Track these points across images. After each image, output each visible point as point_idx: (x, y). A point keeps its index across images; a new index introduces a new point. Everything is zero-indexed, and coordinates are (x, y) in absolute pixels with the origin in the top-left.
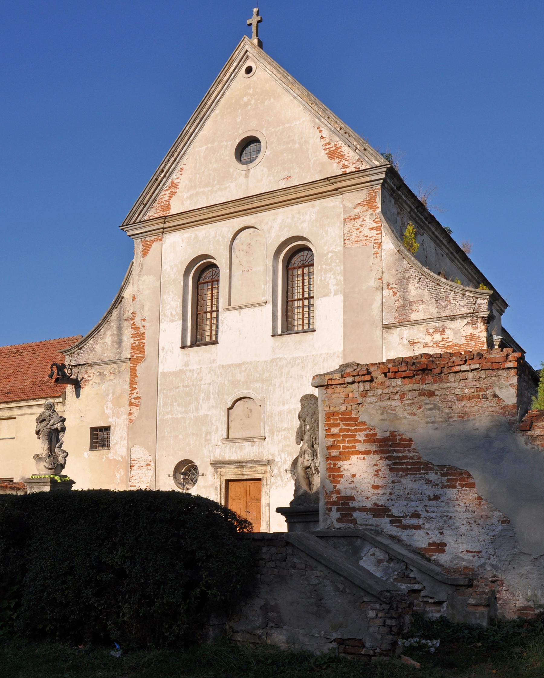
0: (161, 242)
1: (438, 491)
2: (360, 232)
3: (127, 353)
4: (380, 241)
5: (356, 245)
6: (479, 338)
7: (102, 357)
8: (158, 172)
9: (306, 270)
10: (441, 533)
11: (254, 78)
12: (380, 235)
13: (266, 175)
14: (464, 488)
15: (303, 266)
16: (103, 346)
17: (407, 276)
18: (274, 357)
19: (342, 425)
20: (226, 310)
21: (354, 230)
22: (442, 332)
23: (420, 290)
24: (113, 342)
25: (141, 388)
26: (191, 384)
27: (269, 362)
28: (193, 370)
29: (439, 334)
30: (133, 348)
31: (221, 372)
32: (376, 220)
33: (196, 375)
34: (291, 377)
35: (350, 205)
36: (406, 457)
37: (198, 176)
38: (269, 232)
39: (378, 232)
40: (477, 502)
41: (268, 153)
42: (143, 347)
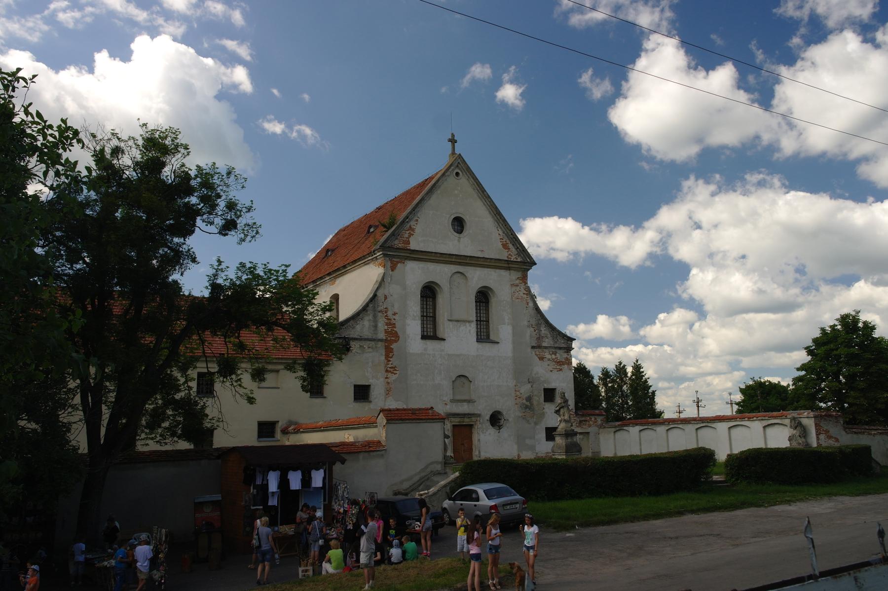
3: (382, 335)
16: (363, 328)
25: (394, 361)
30: (386, 331)
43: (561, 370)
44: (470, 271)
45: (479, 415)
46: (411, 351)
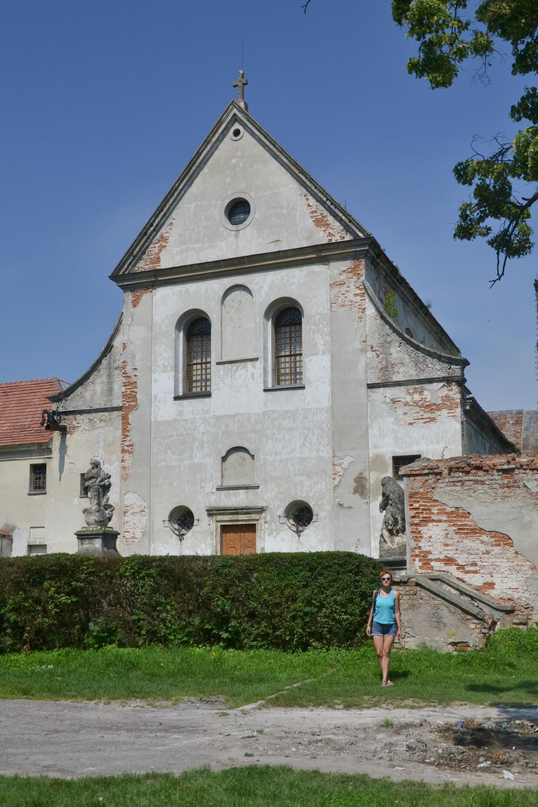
0: (151, 294)
1: (489, 548)
2: (346, 297)
4: (364, 307)
5: (342, 309)
6: (453, 399)
7: (92, 405)
8: (148, 226)
9: (293, 328)
10: (492, 576)
11: (242, 141)
12: (364, 301)
13: (255, 237)
14: (506, 546)
15: (291, 324)
16: (93, 393)
17: (389, 341)
18: (266, 410)
19: (421, 502)
20: (218, 364)
21: (340, 295)
22: (421, 393)
23: (400, 354)
24: (103, 390)
25: (134, 436)
26: (185, 433)
27: (261, 414)
28: (187, 420)
29: (418, 394)
30: (124, 395)
31: (214, 423)
32: (361, 287)
33: (189, 424)
34: (283, 429)
35: (336, 272)
36: (466, 525)
37: (188, 232)
38: (260, 292)
39: (362, 298)
40: (515, 555)
41: (257, 216)
42: (135, 396)
43: (433, 420)
45: (262, 510)
46: (159, 419)
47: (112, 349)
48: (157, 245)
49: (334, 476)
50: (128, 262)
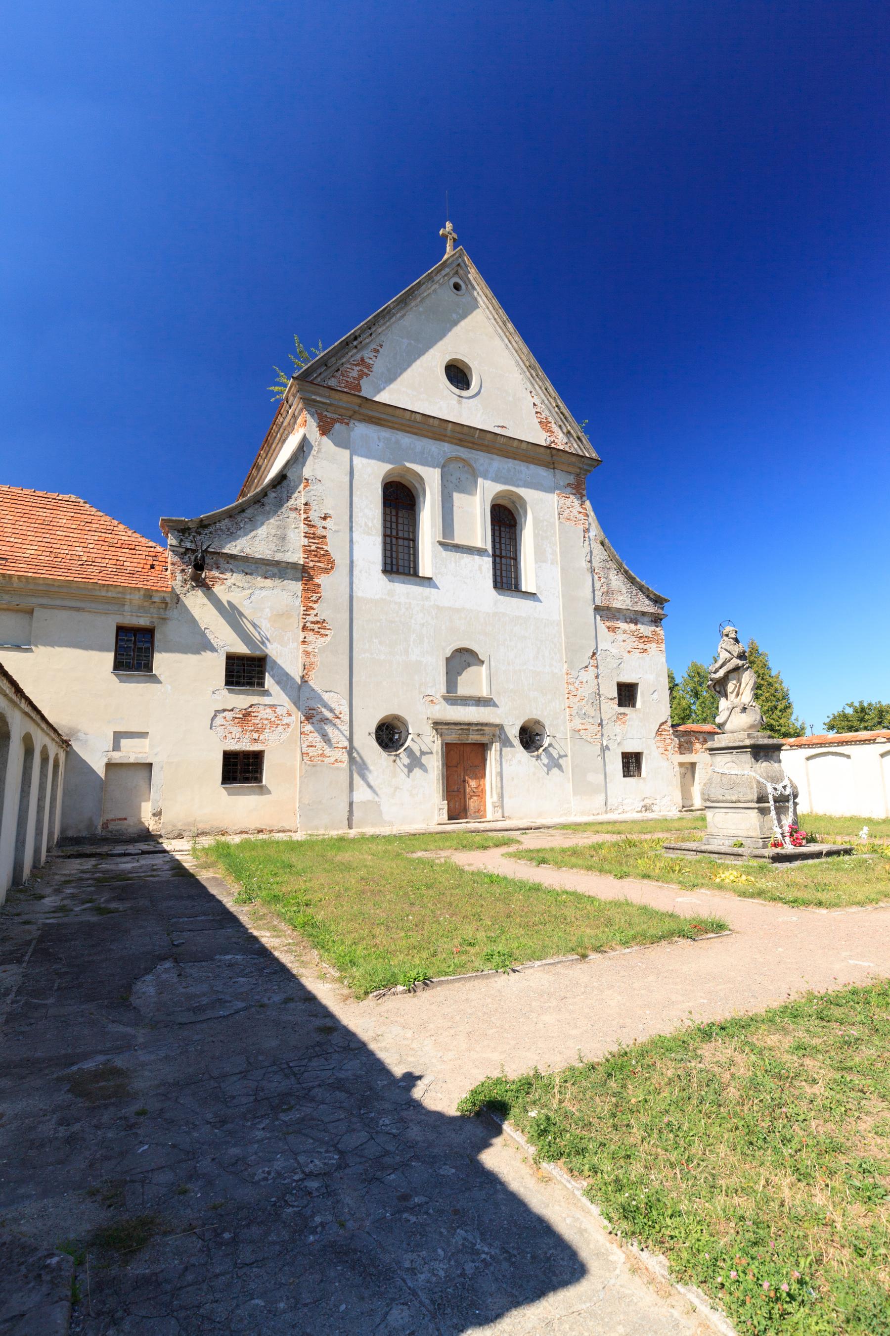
5: (568, 523)
23: (618, 583)
25: (322, 611)
35: (562, 483)
43: (645, 650)
44: (480, 459)
47: (285, 483)
48: (354, 368)
49: (567, 696)
50: (319, 372)
